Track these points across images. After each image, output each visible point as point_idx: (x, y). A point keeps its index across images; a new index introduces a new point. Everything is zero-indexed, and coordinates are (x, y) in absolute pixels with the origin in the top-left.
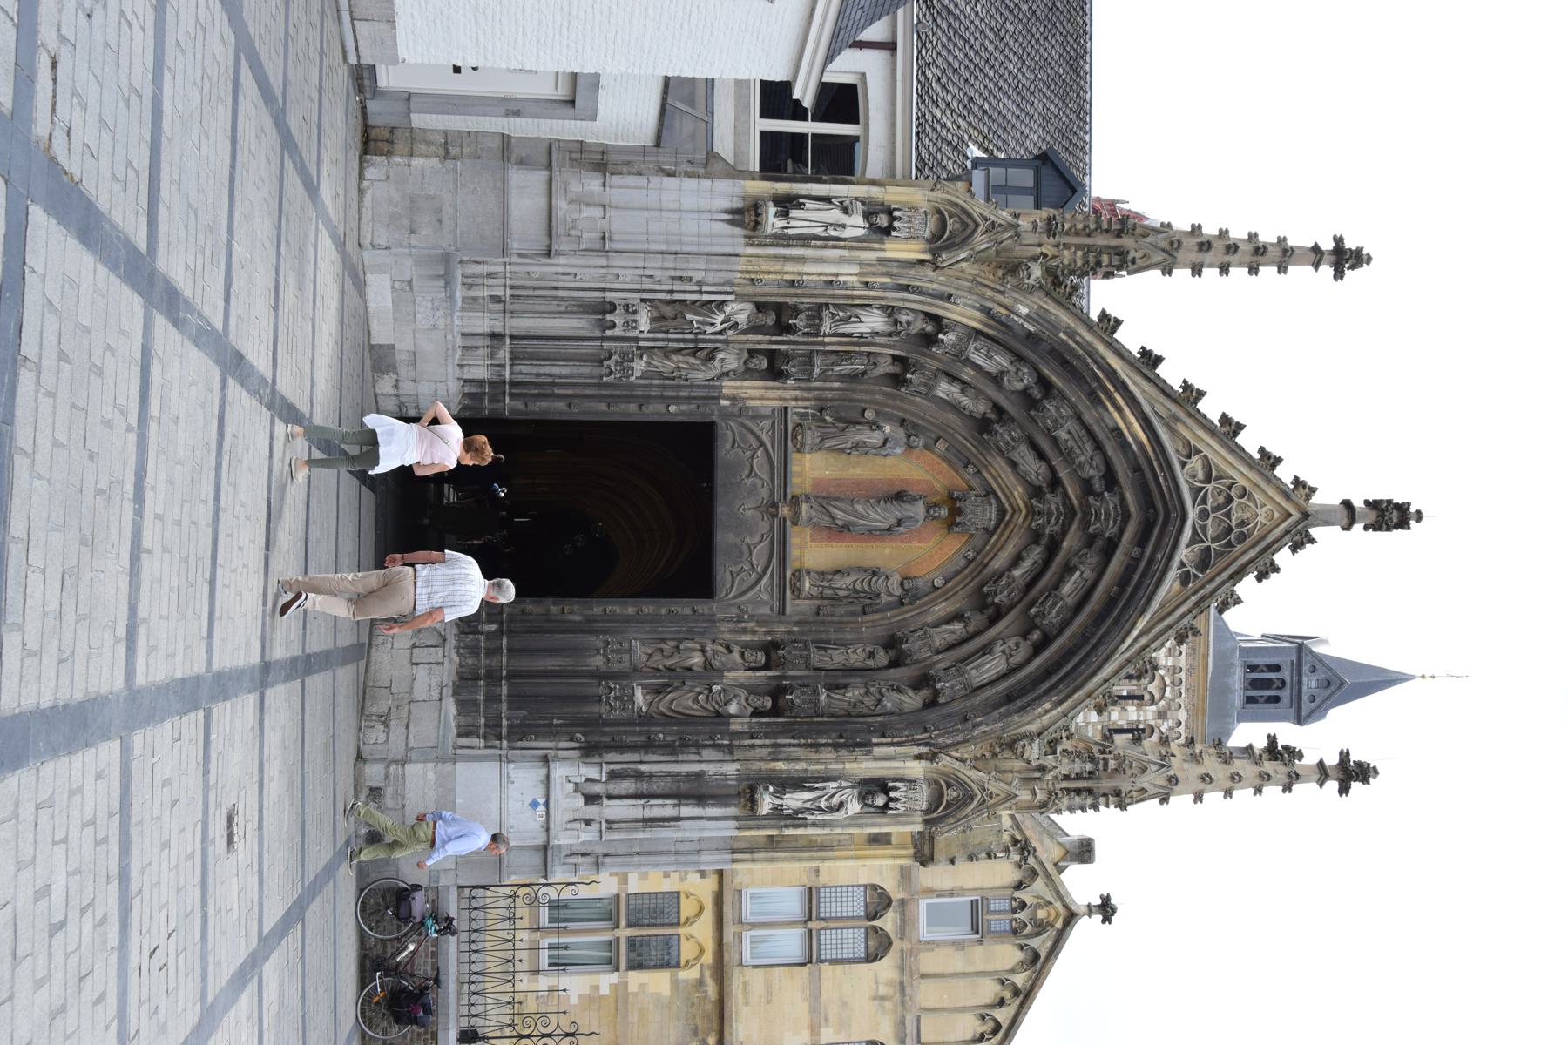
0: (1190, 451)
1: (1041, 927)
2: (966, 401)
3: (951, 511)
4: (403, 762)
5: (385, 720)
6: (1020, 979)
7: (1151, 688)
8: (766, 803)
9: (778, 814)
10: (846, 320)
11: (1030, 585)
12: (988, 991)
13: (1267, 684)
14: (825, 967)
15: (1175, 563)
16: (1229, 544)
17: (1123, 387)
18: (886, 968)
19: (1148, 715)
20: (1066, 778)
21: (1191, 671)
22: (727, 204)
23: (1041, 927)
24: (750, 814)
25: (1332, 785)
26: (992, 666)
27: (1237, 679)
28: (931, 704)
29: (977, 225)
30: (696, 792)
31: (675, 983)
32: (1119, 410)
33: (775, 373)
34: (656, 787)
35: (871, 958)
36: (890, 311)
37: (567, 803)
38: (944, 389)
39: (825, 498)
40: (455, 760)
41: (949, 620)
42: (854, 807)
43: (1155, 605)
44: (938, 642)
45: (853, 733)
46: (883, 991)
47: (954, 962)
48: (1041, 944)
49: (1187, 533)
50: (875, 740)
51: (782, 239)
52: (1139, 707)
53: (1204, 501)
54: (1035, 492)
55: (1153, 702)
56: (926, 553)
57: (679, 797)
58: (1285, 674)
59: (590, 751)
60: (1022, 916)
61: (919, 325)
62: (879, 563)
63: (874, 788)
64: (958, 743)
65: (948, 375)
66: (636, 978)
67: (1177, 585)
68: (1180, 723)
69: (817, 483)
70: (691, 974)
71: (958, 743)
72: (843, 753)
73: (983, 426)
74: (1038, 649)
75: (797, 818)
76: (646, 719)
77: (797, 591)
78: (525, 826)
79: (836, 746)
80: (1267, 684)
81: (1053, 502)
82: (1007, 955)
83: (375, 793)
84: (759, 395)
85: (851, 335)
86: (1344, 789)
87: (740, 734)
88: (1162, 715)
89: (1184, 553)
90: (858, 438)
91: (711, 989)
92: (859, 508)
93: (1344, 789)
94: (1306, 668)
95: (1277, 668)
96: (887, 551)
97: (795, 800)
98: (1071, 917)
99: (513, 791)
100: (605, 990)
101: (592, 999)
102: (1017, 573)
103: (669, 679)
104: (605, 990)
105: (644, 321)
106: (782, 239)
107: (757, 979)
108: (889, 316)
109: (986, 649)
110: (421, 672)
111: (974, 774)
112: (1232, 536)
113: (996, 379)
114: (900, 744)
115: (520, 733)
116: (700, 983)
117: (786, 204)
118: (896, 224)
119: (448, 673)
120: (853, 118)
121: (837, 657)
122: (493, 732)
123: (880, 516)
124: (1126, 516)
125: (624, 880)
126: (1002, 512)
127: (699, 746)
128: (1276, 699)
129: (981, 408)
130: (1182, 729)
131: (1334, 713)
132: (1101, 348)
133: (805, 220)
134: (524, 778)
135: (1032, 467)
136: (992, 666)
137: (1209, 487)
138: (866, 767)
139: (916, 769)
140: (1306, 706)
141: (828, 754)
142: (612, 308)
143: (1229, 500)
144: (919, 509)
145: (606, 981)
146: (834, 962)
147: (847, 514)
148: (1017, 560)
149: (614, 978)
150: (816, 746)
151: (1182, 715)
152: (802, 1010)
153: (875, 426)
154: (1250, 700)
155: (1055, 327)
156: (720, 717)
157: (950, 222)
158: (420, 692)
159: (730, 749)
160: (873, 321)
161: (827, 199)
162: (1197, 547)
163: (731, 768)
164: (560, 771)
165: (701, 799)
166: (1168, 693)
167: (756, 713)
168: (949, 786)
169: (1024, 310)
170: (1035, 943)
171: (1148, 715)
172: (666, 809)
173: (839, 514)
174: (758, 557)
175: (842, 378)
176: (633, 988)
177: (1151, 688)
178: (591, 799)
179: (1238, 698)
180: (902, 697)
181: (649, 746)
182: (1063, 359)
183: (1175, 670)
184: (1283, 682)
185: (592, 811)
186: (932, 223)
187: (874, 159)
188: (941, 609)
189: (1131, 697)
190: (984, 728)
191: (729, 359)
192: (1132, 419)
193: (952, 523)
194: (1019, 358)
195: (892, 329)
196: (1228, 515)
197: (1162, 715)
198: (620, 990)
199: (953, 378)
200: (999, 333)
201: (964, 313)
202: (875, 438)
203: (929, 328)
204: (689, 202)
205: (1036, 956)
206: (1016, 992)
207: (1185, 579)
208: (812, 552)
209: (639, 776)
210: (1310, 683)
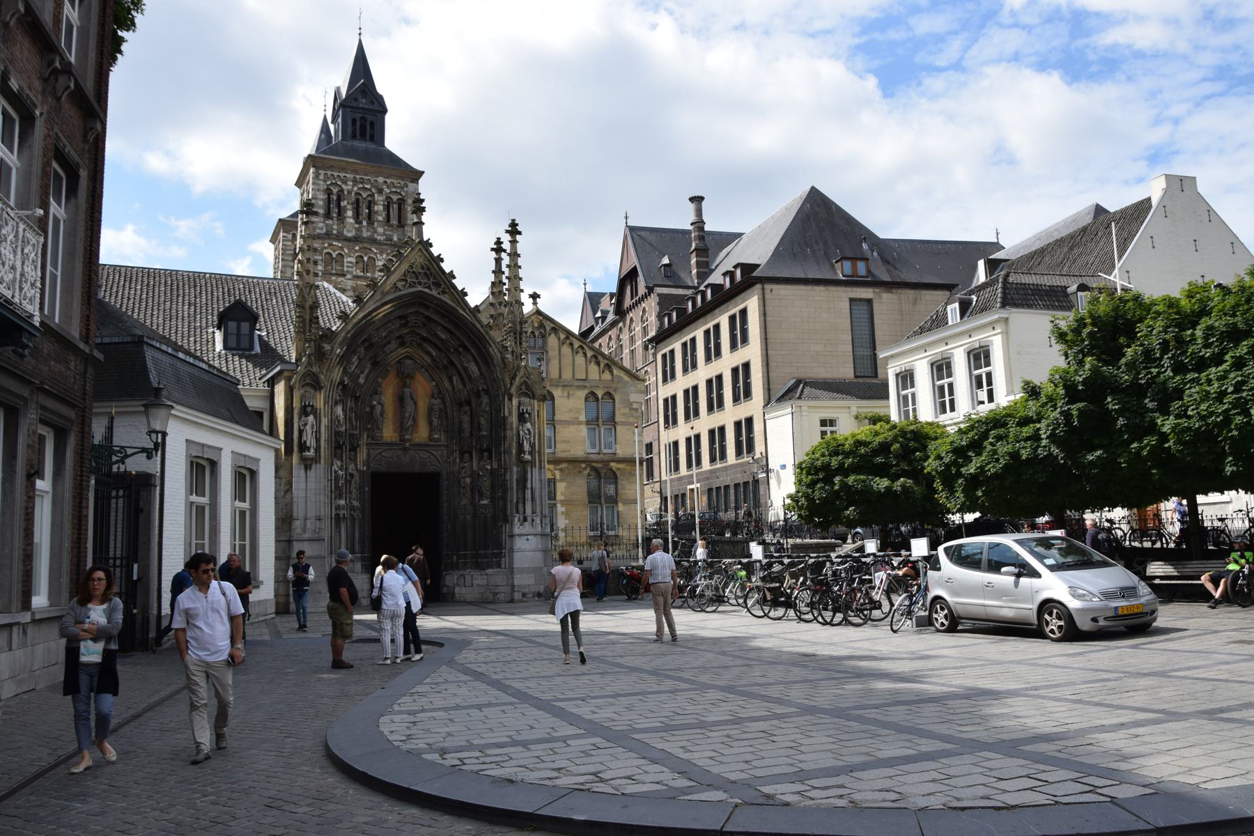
0: (395, 287)
1: (542, 326)
3: (405, 378)
4: (513, 586)
5: (495, 594)
6: (562, 336)
7: (364, 195)
8: (528, 457)
9: (531, 453)
11: (439, 349)
12: (566, 350)
13: (363, 128)
14: (556, 418)
17: (370, 313)
18: (557, 393)
21: (355, 172)
22: (303, 472)
23: (542, 326)
24: (532, 463)
25: (518, 237)
26: (473, 368)
27: (360, 145)
28: (487, 392)
30: (522, 481)
31: (561, 480)
33: (354, 449)
34: (521, 496)
35: (553, 399)
37: (527, 528)
38: (361, 381)
39: (401, 428)
40: (512, 569)
41: (452, 382)
42: (528, 425)
44: (461, 387)
45: (499, 423)
47: (555, 362)
48: (548, 326)
49: (427, 290)
51: (317, 450)
52: (375, 203)
54: (402, 344)
55: (373, 195)
56: (422, 388)
57: (524, 488)
58: (358, 116)
59: (506, 520)
60: (537, 333)
63: (522, 418)
66: (559, 497)
69: (395, 431)
70: (558, 474)
72: (508, 426)
74: (466, 349)
75: (532, 446)
76: (493, 499)
77: (438, 440)
78: (534, 542)
79: (505, 430)
80: (363, 128)
81: (408, 339)
82: (552, 341)
83: (524, 595)
84: (362, 455)
86: (520, 233)
87: (500, 466)
88: (380, 191)
91: (564, 466)
93: (520, 233)
94: (355, 104)
95: (354, 121)
97: (527, 447)
98: (538, 312)
99: (523, 547)
100: (563, 509)
101: (567, 514)
103: (476, 490)
104: (563, 509)
105: (342, 502)
106: (317, 450)
107: (560, 447)
109: (466, 369)
110: (475, 582)
115: (499, 546)
116: (561, 470)
117: (303, 447)
119: (476, 573)
121: (466, 426)
122: (500, 556)
123: (410, 408)
126: (407, 357)
127: (505, 480)
128: (372, 124)
130: (389, 181)
131: (381, 88)
132: (355, 321)
133: (310, 440)
134: (519, 543)
135: (393, 345)
136: (473, 368)
138: (514, 419)
139: (515, 402)
140: (376, 107)
141: (509, 433)
142: (337, 515)
144: (406, 390)
145: (560, 509)
146: (554, 414)
147: (411, 422)
148: (428, 353)
149: (559, 505)
150: (505, 437)
151: (381, 180)
152: (572, 428)
153: (373, 407)
154: (372, 139)
155: (345, 338)
156: (492, 472)
158: (485, 582)
159: (506, 469)
160: (339, 410)
161: (301, 432)
163: (515, 469)
164: (516, 531)
165: (525, 480)
167: (490, 458)
170: (548, 329)
171: (379, 198)
172: (528, 492)
174: (424, 455)
176: (562, 498)
177: (364, 195)
178: (525, 520)
179: (371, 146)
181: (505, 499)
182: (355, 336)
183: (355, 181)
184: (362, 118)
185: (529, 519)
186: (308, 389)
188: (446, 384)
189: (369, 207)
191: (352, 467)
193: (411, 377)
194: (354, 352)
197: (380, 191)
198: (563, 503)
200: (344, 359)
202: (379, 408)
204: (303, 486)
205: (553, 328)
206: (567, 338)
207: (444, 292)
208: (422, 433)
209: (517, 503)
210: (363, 102)
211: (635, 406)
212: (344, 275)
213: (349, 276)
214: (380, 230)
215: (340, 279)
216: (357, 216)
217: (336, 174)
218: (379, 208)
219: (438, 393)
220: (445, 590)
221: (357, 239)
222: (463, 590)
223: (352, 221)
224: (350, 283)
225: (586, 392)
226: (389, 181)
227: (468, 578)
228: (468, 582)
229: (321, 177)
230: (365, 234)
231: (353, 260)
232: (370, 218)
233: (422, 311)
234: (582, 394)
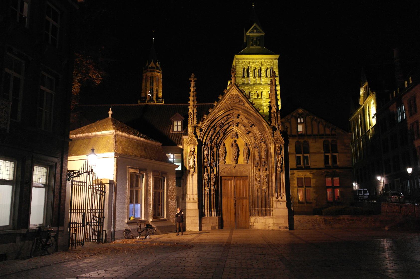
12: (314, 122)
19: (263, 68)
31: (312, 178)
46: (314, 141)
62: (243, 149)
68: (265, 61)
70: (311, 176)
88: (262, 65)
91: (314, 171)
116: (313, 174)
119: (261, 218)
121: (257, 157)
125: (295, 187)
130: (266, 61)
158: (264, 221)
166: (258, 64)
171: (263, 68)
176: (314, 186)
211: (347, 145)
214: (263, 80)
216: (255, 76)
217: (245, 61)
218: (263, 71)
220: (250, 224)
221: (254, 84)
222: (257, 224)
223: (252, 78)
225: (323, 140)
226: (266, 61)
227: (258, 219)
228: (258, 222)
229: (240, 63)
230: (258, 82)
232: (260, 76)
234: (322, 141)
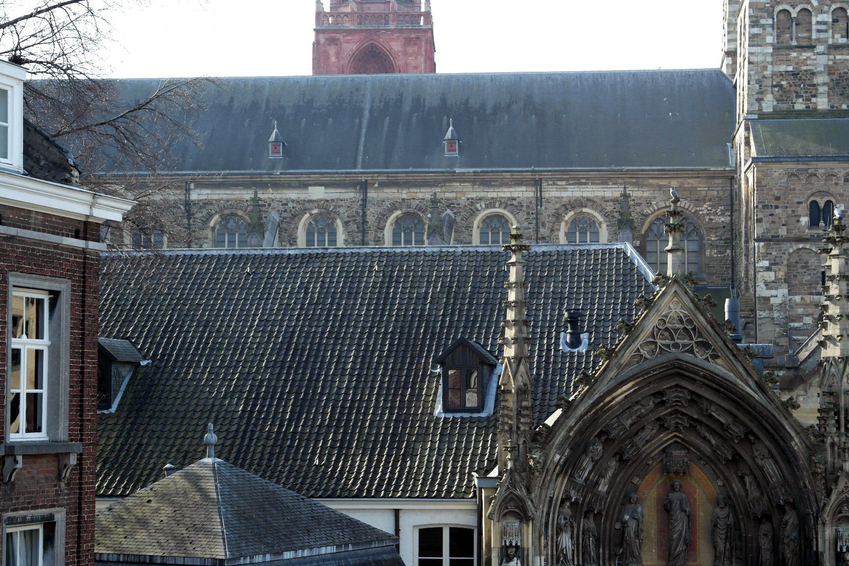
2: (610, 474)
10: (565, 556)
11: (720, 436)
15: (705, 364)
16: (694, 329)
17: (601, 399)
20: (838, 429)
26: (769, 467)
28: (793, 506)
29: (511, 493)
32: (613, 399)
36: (559, 530)
38: (603, 488)
41: (744, 484)
43: (731, 376)
44: (757, 494)
49: (688, 357)
50: (815, 549)
53: (668, 346)
54: (663, 428)
56: (702, 489)
61: (567, 510)
64: (816, 498)
65: (594, 486)
67: (719, 361)
71: (816, 498)
73: (623, 462)
81: (671, 422)
85: (573, 551)
89: (699, 358)
90: (632, 536)
92: (675, 536)
96: (702, 514)
102: (713, 442)
108: (562, 530)
109: (761, 469)
111: (833, 497)
112: (689, 327)
113: (596, 463)
114: (817, 534)
118: (514, 544)
120: (441, 529)
123: (680, 525)
124: (677, 386)
129: (613, 464)
135: (647, 433)
136: (769, 467)
137: (659, 342)
139: (829, 532)
143: (667, 329)
144: (674, 496)
153: (624, 524)
155: (567, 438)
157: (510, 508)
160: (566, 541)
162: (696, 350)
168: (840, 512)
169: (558, 457)
173: (679, 548)
175: (597, 547)
180: (790, 524)
187: (466, 520)
188: (736, 486)
190: (807, 483)
192: (620, 391)
193: (685, 472)
194: (585, 451)
195: (569, 528)
196: (676, 330)
199: (597, 483)
200: (570, 466)
201: (559, 488)
202: (632, 525)
203: (568, 504)
212: (812, 47)
213: (820, 48)
215: (805, 55)
219: (728, 501)
224: (823, 60)
231: (828, 18)
233: (685, 384)
